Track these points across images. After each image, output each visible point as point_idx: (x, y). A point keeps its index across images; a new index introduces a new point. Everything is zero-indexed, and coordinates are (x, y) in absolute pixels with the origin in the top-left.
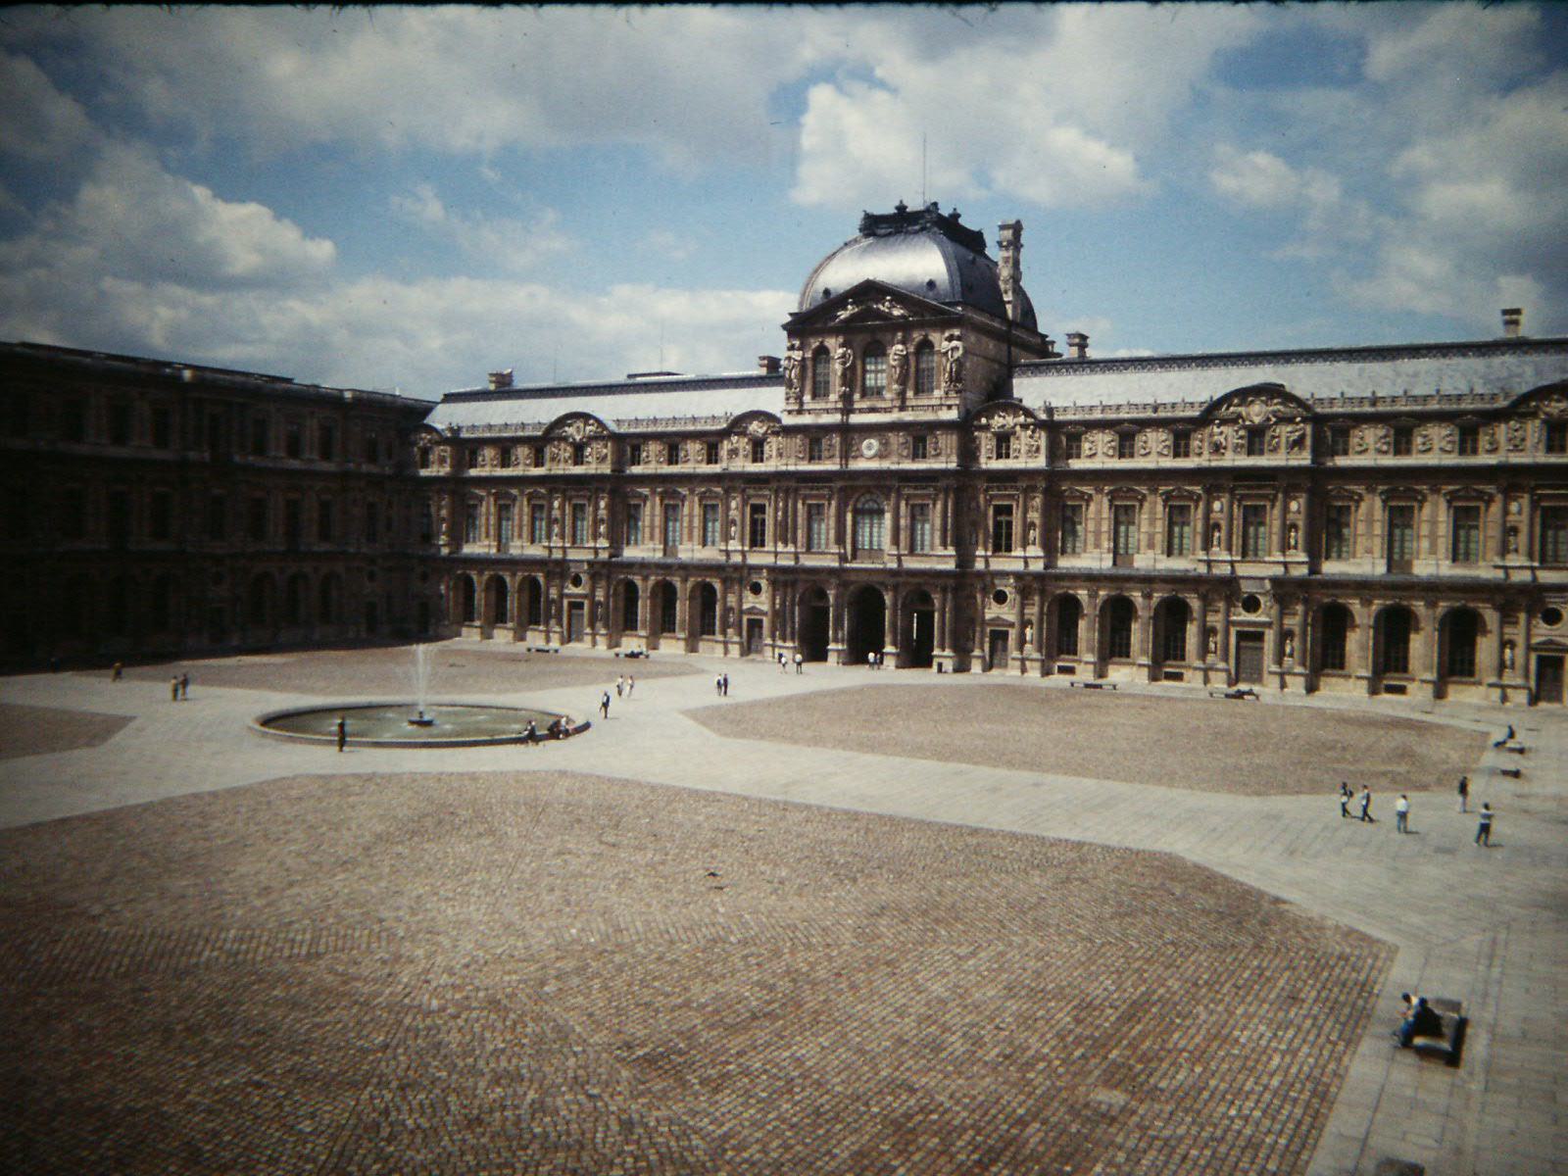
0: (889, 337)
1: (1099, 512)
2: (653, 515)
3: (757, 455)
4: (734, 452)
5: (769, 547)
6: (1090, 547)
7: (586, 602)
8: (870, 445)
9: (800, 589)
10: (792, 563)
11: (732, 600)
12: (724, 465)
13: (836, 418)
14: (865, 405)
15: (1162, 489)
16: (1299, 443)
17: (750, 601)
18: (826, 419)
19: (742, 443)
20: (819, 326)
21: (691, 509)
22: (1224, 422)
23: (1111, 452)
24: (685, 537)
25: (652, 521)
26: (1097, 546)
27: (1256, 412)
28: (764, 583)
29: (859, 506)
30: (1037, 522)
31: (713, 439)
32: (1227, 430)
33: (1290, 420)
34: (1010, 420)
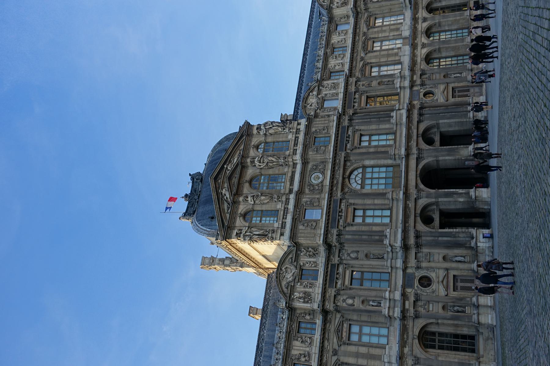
1: (376, 57)
4: (307, 297)
6: (397, 58)
8: (316, 179)
9: (421, 227)
10: (400, 231)
11: (436, 309)
12: (315, 306)
13: (292, 197)
14: (288, 183)
15: (365, 30)
18: (291, 206)
20: (228, 215)
26: (396, 54)
28: (419, 274)
29: (359, 187)
30: (379, 81)
31: (295, 326)
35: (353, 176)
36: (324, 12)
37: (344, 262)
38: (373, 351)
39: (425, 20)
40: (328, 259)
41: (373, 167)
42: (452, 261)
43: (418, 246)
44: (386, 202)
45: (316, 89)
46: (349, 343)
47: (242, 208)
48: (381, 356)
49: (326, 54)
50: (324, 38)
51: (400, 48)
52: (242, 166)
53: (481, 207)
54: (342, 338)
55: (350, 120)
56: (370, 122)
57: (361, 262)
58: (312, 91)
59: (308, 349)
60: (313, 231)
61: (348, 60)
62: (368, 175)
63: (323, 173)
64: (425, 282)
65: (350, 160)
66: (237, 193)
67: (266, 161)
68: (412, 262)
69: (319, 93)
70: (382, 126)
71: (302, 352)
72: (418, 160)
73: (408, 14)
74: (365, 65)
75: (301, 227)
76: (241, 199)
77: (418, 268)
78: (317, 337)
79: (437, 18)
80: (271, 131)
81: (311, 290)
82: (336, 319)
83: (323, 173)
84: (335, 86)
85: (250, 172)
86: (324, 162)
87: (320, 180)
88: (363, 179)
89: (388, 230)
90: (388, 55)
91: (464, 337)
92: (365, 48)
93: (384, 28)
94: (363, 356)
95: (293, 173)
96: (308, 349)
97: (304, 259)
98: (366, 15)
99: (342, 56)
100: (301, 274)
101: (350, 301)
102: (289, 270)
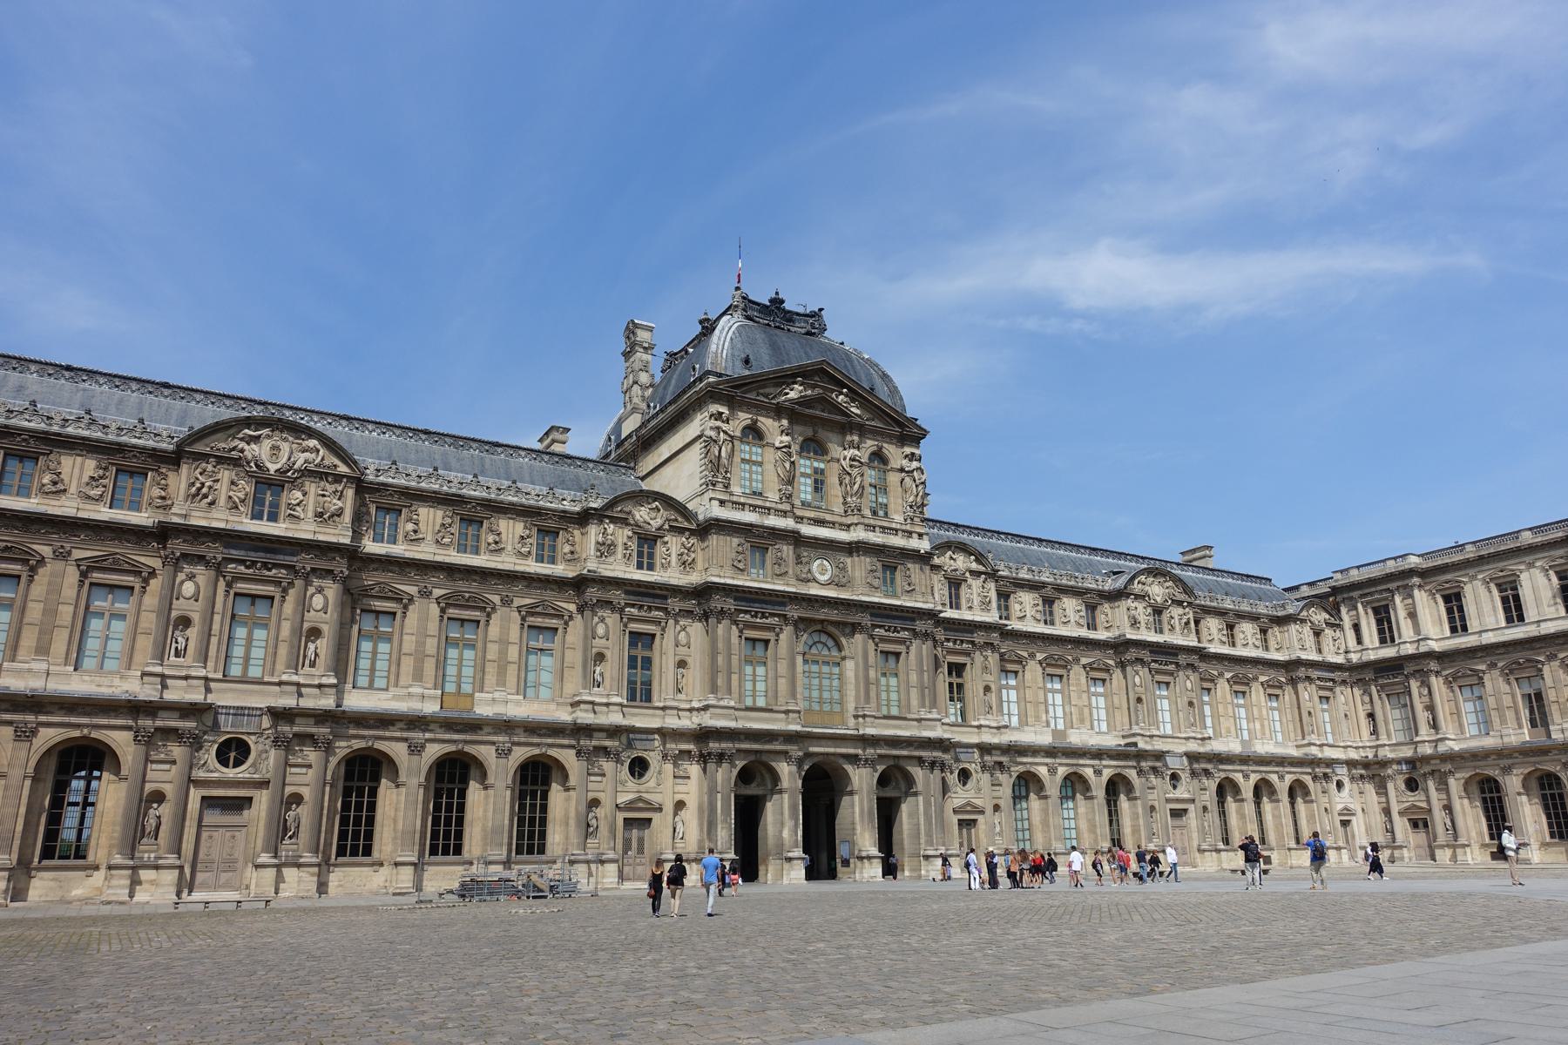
0: (834, 437)
2: (423, 634)
3: (646, 560)
4: (606, 549)
7: (262, 799)
8: (822, 569)
10: (732, 724)
12: (592, 565)
14: (812, 514)
16: (1187, 623)
19: (621, 535)
21: (505, 626)
22: (1138, 597)
23: (1038, 616)
24: (491, 678)
25: (421, 644)
26: (1037, 718)
27: (1158, 591)
28: (653, 758)
31: (551, 524)
32: (1140, 606)
33: (1180, 603)
34: (962, 562)
35: (824, 638)
36: (1120, 582)
37: (671, 622)
38: (512, 671)
40: (676, 591)
41: (841, 677)
42: (675, 814)
43: (704, 759)
44: (781, 700)
45: (981, 568)
47: (768, 424)
48: (504, 685)
49: (1043, 585)
50: (1072, 583)
51: (1048, 725)
52: (846, 426)
53: (770, 868)
54: (533, 614)
56: (922, 671)
57: (671, 652)
58: (977, 560)
59: (509, 548)
60: (729, 563)
61: (1031, 629)
62: (825, 669)
63: (829, 583)
64: (639, 767)
65: (852, 634)
67: (855, 472)
69: (972, 572)
70: (914, 693)
71: (504, 536)
73: (1111, 741)
75: (736, 541)
76: (785, 422)
77: (665, 757)
78: (532, 567)
79: (1099, 792)
80: (907, 479)
81: (620, 556)
83: (829, 583)
84: (986, 605)
87: (818, 576)
89: (732, 703)
91: (543, 835)
93: (1085, 696)
94: (503, 653)
95: (832, 525)
96: (509, 548)
97: (674, 544)
98: (1111, 662)
99: (1038, 616)
101: (601, 630)
102: (653, 514)
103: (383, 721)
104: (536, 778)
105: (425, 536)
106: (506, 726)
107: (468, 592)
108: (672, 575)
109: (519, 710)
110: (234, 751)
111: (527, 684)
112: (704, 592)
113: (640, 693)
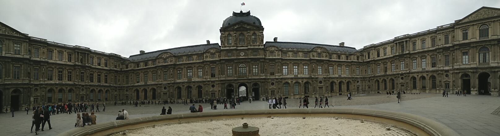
4: (207, 57)
5: (216, 76)
8: (242, 54)
9: (226, 84)
11: (207, 89)
13: (235, 48)
17: (212, 89)
18: (232, 48)
19: (208, 55)
39: (302, 81)
40: (217, 61)
46: (198, 69)
47: (232, 33)
52: (247, 30)
55: (264, 62)
64: (213, 86)
66: (237, 30)
68: (217, 83)
72: (247, 82)
73: (307, 76)
74: (288, 64)
78: (198, 61)
82: (203, 65)
84: (278, 55)
85: (245, 33)
86: (248, 55)
88: (242, 67)
90: (291, 71)
92: (295, 63)
97: (217, 54)
100: (213, 54)
103: (180, 83)
104: (200, 87)
105: (185, 61)
106: (194, 82)
107: (189, 66)
108: (217, 59)
109: (197, 80)
110: (165, 88)
111: (198, 76)
112: (221, 60)
113: (213, 76)
